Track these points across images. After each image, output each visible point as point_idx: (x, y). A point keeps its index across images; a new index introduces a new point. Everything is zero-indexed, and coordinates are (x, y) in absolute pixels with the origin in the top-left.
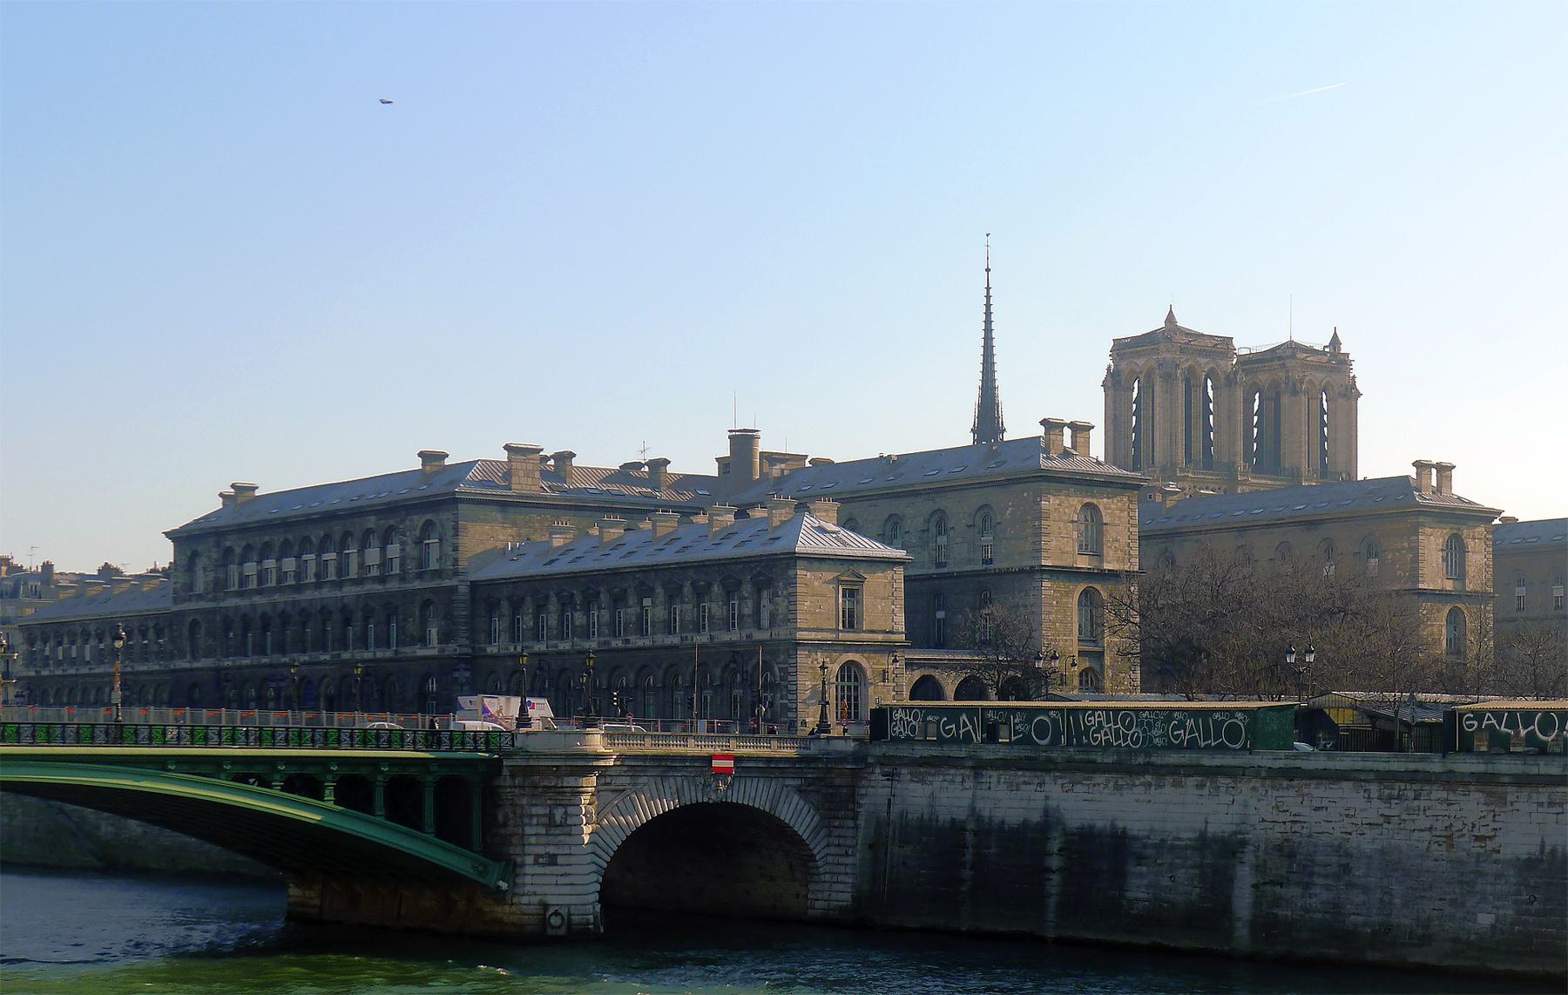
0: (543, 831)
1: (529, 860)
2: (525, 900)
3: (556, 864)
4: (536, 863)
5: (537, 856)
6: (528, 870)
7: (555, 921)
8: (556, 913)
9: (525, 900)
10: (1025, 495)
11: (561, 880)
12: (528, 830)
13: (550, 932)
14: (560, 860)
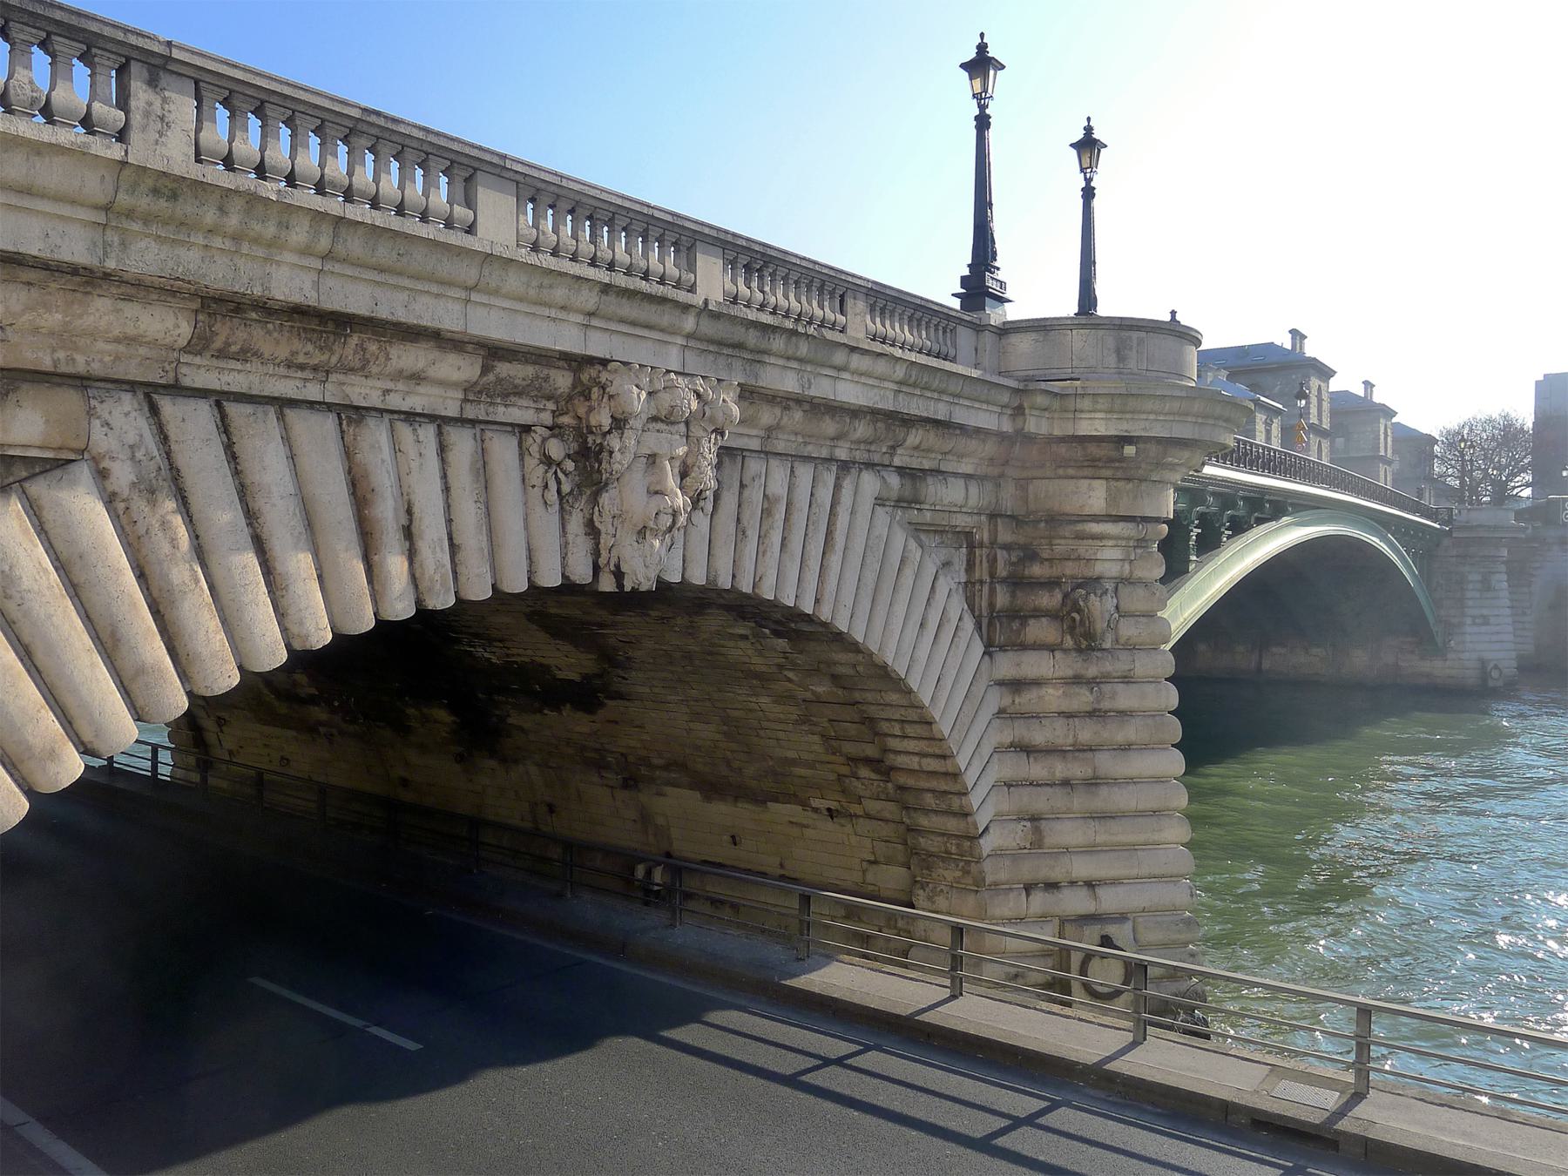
0: (1478, 595)
1: (1469, 621)
2: (1466, 656)
3: (1486, 623)
4: (1474, 624)
5: (1474, 617)
6: (1468, 629)
7: (1495, 674)
8: (1496, 667)
9: (1466, 656)
10: (1294, 377)
11: (1494, 638)
12: (1469, 594)
13: (1491, 684)
14: (1492, 620)
